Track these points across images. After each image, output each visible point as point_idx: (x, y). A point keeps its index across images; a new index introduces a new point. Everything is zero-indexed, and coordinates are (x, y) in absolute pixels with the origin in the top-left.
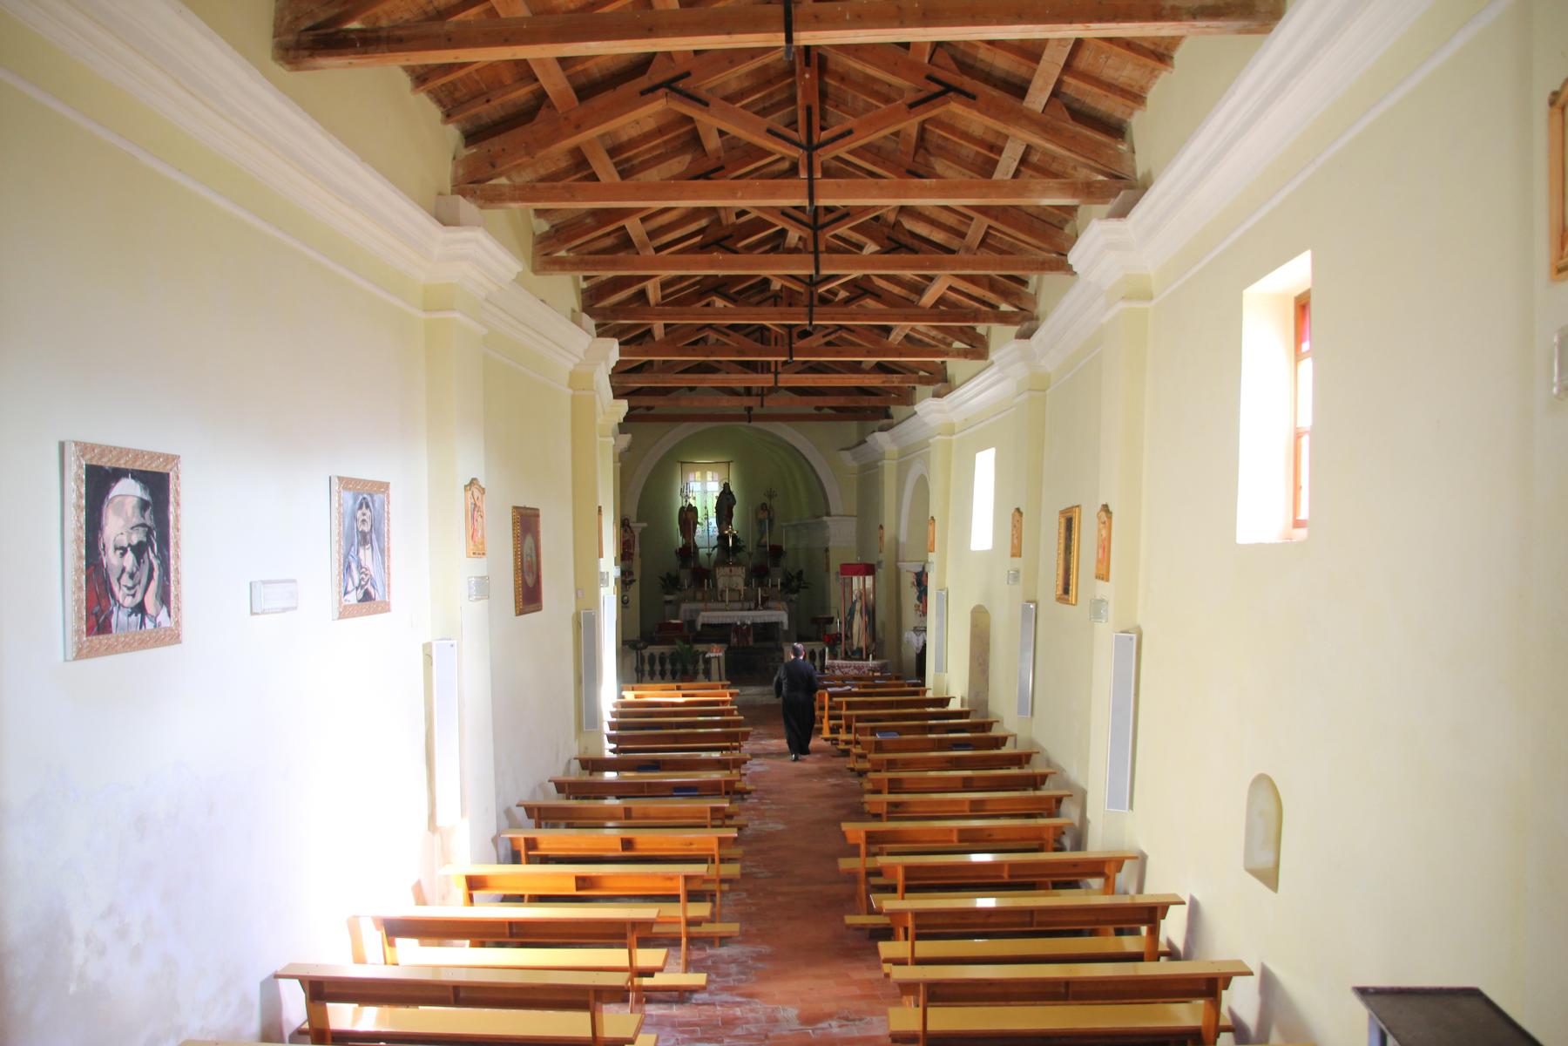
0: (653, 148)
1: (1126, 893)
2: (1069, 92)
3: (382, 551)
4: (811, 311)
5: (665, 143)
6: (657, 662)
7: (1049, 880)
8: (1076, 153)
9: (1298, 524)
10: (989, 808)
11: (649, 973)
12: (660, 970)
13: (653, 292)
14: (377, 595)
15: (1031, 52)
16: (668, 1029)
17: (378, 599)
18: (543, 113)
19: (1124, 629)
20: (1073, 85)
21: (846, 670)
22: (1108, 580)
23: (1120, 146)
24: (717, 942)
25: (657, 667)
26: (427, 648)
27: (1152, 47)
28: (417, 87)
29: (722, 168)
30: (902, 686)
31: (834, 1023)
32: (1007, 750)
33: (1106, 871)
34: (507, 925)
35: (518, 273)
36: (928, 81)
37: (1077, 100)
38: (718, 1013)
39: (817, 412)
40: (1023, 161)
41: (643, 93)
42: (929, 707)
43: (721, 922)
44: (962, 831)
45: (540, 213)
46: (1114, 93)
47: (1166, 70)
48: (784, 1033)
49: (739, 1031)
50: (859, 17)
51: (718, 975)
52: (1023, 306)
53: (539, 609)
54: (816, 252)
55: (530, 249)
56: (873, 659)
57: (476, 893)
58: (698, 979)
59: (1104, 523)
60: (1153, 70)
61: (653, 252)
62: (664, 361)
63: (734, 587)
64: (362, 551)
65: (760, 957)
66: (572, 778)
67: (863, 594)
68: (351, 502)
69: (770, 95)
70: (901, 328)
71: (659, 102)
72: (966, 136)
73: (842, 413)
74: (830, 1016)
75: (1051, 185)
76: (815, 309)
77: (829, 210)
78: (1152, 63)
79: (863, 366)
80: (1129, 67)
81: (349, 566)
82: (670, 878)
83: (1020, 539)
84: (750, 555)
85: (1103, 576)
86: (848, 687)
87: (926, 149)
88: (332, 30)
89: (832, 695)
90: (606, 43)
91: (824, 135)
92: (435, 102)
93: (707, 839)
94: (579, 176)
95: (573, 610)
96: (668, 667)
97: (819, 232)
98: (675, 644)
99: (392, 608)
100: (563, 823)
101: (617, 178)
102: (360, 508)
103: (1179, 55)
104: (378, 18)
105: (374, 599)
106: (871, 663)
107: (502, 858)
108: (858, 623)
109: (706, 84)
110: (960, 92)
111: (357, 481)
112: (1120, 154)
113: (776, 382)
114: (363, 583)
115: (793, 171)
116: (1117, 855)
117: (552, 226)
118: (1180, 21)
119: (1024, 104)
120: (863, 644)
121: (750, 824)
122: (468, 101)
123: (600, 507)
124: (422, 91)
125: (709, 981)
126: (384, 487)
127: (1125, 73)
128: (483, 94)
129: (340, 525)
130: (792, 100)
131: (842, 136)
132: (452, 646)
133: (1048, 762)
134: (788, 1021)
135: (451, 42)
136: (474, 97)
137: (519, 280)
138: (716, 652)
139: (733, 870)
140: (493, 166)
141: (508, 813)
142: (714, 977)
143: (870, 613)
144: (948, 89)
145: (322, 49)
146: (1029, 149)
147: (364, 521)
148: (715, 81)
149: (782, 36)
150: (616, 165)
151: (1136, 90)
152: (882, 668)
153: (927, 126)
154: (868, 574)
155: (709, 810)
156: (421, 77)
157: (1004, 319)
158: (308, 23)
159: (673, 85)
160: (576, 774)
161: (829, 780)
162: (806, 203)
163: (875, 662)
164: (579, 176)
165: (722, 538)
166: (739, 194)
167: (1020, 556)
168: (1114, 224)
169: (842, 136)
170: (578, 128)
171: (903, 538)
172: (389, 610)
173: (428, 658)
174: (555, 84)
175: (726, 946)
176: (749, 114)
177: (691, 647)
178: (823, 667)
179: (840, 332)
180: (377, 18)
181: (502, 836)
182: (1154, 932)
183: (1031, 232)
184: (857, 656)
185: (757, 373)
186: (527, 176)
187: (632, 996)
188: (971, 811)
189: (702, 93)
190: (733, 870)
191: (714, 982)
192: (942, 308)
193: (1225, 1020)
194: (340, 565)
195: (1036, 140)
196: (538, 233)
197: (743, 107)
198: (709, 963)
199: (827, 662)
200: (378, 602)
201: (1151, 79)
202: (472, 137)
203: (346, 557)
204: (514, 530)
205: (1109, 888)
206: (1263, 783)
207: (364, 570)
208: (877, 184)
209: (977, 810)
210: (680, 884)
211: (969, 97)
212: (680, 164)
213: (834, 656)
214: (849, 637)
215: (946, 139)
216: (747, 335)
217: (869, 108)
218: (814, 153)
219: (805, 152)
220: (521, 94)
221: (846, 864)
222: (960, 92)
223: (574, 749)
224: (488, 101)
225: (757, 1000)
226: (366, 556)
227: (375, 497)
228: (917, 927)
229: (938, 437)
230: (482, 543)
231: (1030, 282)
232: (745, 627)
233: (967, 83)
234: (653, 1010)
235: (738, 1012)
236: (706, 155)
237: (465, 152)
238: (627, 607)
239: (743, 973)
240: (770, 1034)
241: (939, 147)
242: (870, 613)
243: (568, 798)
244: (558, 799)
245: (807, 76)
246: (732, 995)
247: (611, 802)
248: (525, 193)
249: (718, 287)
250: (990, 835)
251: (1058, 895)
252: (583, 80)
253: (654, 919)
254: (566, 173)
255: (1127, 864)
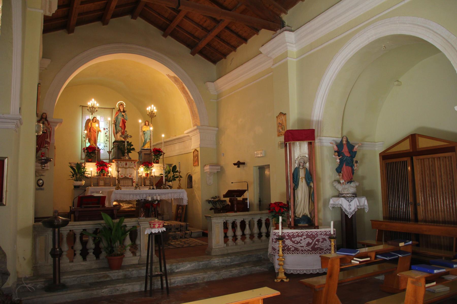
6: (78, 240)
21: (298, 239)
96: (91, 245)
98: (102, 219)
138: (159, 227)
177: (121, 222)
232: (157, 202)
238: (42, 189)
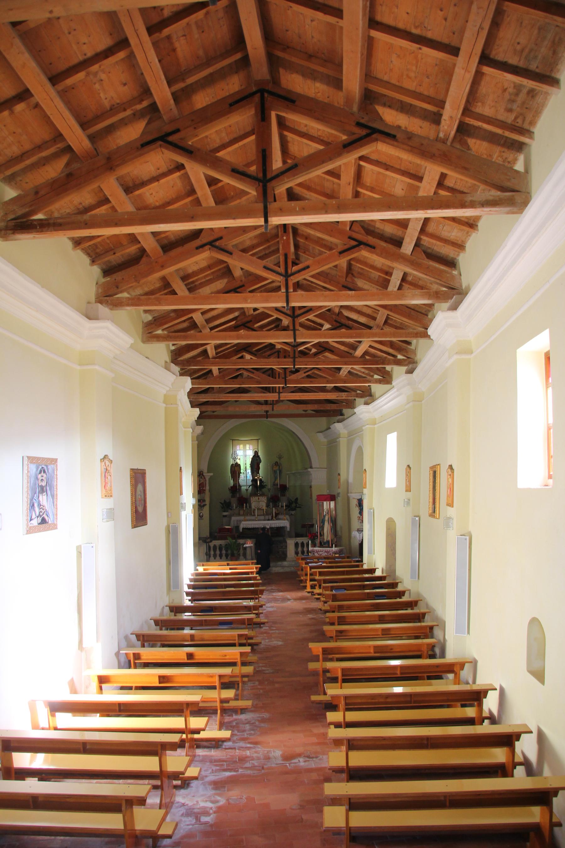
0: (207, 276)
1: (467, 683)
2: (425, 244)
3: (53, 496)
4: (294, 361)
5: (212, 273)
6: (218, 549)
7: (425, 675)
8: (430, 276)
9: (550, 477)
10: (392, 633)
11: (198, 731)
12: (204, 730)
13: (211, 352)
14: (50, 520)
15: (403, 224)
16: (208, 763)
17: (50, 522)
18: (144, 259)
19: (462, 533)
20: (426, 241)
21: (321, 553)
22: (453, 507)
23: (454, 272)
24: (239, 711)
25: (218, 552)
26: (79, 549)
27: (466, 220)
28: (75, 247)
29: (243, 286)
30: (350, 562)
31: (301, 760)
32: (405, 599)
33: (455, 669)
34: (117, 705)
35: (132, 344)
36: (349, 239)
37: (429, 248)
38: (237, 754)
39: (304, 412)
40: (404, 279)
41: (197, 248)
42: (365, 574)
43: (241, 700)
44: (375, 647)
45: (146, 311)
46: (449, 245)
47: (474, 232)
48: (273, 765)
49: (248, 765)
50: (304, 209)
51: (238, 731)
52: (409, 356)
53: (146, 524)
54: (294, 330)
55: (141, 331)
56: (335, 547)
57: (104, 686)
58: (226, 734)
59: (450, 475)
60: (468, 232)
61: (209, 330)
62: (220, 387)
63: (261, 507)
64: (41, 496)
65: (263, 720)
66: (165, 618)
67: (329, 510)
68: (35, 470)
69: (269, 247)
70: (346, 369)
71: (207, 252)
72: (373, 267)
73: (319, 413)
74: (299, 755)
75: (416, 293)
76: (296, 359)
77: (300, 308)
78: (466, 229)
79: (327, 388)
80: (455, 230)
81: (33, 505)
82: (212, 676)
83: (410, 482)
84: (269, 490)
85: (450, 504)
86: (320, 563)
87: (352, 274)
88: (25, 220)
89: (311, 568)
90: (169, 225)
91: (295, 268)
92: (86, 255)
93: (233, 653)
94: (166, 291)
95: (166, 524)
96: (224, 552)
97: (296, 319)
98: (228, 540)
99: (59, 527)
100: (159, 644)
101: (187, 293)
102: (40, 473)
103: (481, 224)
104: (52, 213)
105: (48, 523)
106: (334, 549)
107: (122, 664)
108: (327, 527)
109: (230, 244)
110: (367, 245)
111: (38, 459)
112: (453, 277)
113: (279, 398)
114: (41, 514)
115: (278, 289)
116: (460, 661)
117: (154, 318)
118: (475, 208)
119: (401, 251)
120: (329, 539)
121: (263, 642)
122: (104, 253)
123: (181, 468)
124: (79, 249)
125: (232, 735)
126: (54, 461)
127: (453, 234)
128: (112, 250)
129: (28, 482)
130: (277, 251)
131: (304, 269)
132: (92, 547)
133: (427, 606)
134: (275, 758)
135: (87, 225)
136: (107, 252)
137: (132, 346)
139: (249, 670)
140: (117, 288)
141: (126, 637)
142: (236, 732)
143: (334, 521)
144: (360, 243)
145: (20, 230)
146: (405, 275)
147: (42, 480)
148: (235, 241)
149: (263, 220)
150: (186, 285)
151: (460, 242)
152: (340, 552)
153: (352, 262)
154: (332, 500)
155: (237, 636)
156: (77, 242)
157: (399, 363)
158: (12, 216)
159: (213, 244)
160: (168, 615)
161: (309, 615)
162: (285, 305)
163: (336, 549)
164: (166, 291)
165: (254, 481)
166: (249, 301)
167: (410, 491)
168: (451, 314)
169: (304, 269)
170: (163, 267)
171: (351, 480)
172: (56, 528)
173: (79, 553)
174: (150, 245)
175: (245, 714)
176: (254, 258)
177: (236, 541)
178: (308, 552)
179: (313, 370)
180: (52, 212)
181: (121, 652)
182: (480, 705)
183: (409, 317)
184: (327, 545)
185: (270, 393)
186: (138, 291)
187: (187, 745)
188: (382, 635)
189: (230, 248)
190: (249, 670)
191: (236, 735)
192: (367, 357)
193: (519, 758)
194: (27, 504)
195: (408, 270)
196: (145, 321)
197: (251, 255)
198: (234, 724)
199: (310, 549)
200: (50, 524)
201: (467, 237)
202: (107, 272)
203: (32, 500)
204: (131, 481)
205: (457, 681)
206: (534, 622)
207: (42, 507)
208: (323, 294)
209: (386, 634)
210: (217, 679)
211: (372, 247)
212: (221, 284)
213: (314, 545)
214: (322, 535)
215: (363, 269)
216: (264, 373)
217: (321, 253)
218: (289, 278)
219: (284, 278)
220: (133, 249)
221: (312, 666)
222: (367, 245)
223: (166, 601)
224: (114, 254)
225: (259, 746)
226: (43, 499)
227: (49, 467)
228: (346, 704)
229: (367, 426)
230: (111, 490)
231: (413, 343)
233: (371, 240)
234: (200, 752)
235: (248, 753)
236: (235, 279)
237: (103, 280)
238: (202, 519)
239: (253, 730)
240: (265, 767)
241: (359, 273)
242: (334, 521)
243: (161, 629)
244: (156, 630)
245: (285, 238)
246: (245, 743)
247: (187, 631)
248: (135, 302)
249: (247, 348)
250: (392, 649)
251: (430, 685)
252: (166, 242)
253: (199, 701)
254: (159, 290)
255: (467, 665)
